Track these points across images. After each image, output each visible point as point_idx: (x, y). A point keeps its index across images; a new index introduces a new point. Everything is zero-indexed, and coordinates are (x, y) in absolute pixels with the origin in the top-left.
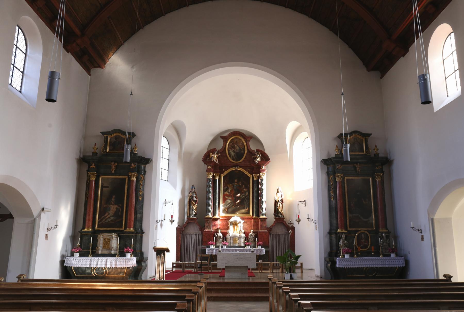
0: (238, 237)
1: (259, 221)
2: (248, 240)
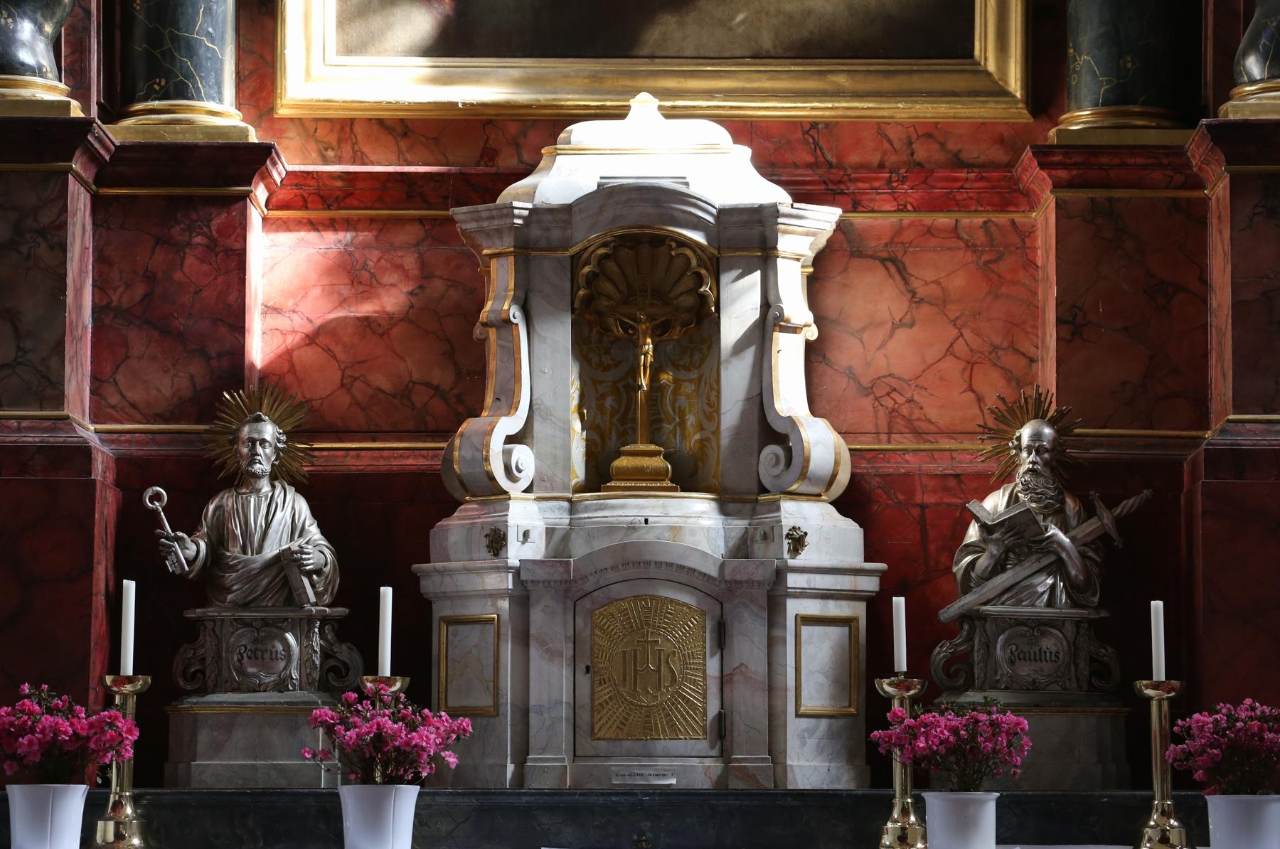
0: (685, 575)
1: (1197, 215)
2: (941, 652)
